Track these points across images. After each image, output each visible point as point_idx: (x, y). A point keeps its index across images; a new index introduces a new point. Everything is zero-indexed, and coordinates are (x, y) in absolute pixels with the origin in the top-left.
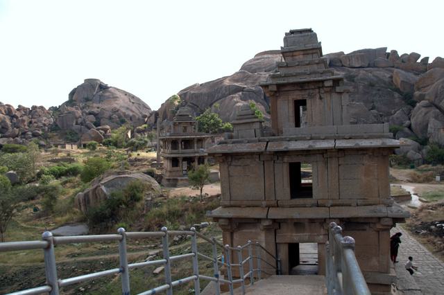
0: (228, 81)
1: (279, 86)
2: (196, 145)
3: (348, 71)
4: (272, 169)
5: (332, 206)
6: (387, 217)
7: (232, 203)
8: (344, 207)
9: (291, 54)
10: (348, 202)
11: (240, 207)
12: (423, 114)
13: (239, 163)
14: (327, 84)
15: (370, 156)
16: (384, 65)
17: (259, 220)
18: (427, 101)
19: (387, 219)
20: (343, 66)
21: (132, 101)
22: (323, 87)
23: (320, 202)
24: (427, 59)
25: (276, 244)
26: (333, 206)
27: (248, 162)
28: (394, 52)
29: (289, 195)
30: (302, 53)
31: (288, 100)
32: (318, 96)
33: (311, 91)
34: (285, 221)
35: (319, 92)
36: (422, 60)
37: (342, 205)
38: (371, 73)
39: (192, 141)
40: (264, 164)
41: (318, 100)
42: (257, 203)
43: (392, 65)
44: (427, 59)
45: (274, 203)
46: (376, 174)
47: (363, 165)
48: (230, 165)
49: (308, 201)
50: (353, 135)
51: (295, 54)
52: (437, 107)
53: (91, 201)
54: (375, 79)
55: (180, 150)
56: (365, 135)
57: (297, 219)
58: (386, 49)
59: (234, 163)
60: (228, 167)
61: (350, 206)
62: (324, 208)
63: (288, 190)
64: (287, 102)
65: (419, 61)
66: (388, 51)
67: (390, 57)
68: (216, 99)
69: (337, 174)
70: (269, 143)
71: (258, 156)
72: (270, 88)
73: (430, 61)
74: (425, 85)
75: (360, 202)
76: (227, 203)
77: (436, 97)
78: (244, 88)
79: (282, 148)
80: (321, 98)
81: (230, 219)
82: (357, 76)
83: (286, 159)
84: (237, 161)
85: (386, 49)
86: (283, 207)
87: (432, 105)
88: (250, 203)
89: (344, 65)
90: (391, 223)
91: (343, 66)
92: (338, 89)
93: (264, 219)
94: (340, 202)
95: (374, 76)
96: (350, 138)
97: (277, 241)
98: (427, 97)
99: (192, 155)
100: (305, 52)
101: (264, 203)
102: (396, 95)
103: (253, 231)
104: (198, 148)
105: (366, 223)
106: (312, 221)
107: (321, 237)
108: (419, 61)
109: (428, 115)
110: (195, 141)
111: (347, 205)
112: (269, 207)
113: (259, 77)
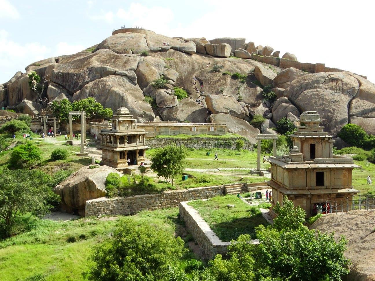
7: (294, 188)
12: (282, 109)
13: (297, 172)
14: (327, 139)
16: (241, 55)
18: (286, 98)
24: (278, 53)
25: (311, 204)
26: (333, 189)
28: (252, 44)
33: (318, 141)
35: (321, 141)
36: (274, 54)
37: (335, 188)
38: (235, 64)
42: (304, 188)
43: (251, 57)
44: (278, 53)
49: (323, 187)
51: (310, 123)
53: (80, 192)
54: (239, 71)
58: (244, 40)
59: (294, 172)
65: (272, 54)
66: (247, 42)
67: (248, 48)
73: (281, 56)
76: (292, 188)
77: (292, 94)
80: (321, 144)
85: (244, 40)
86: (314, 189)
87: (291, 101)
88: (301, 188)
98: (285, 94)
99: (135, 148)
101: (307, 188)
103: (301, 199)
105: (343, 195)
106: (325, 194)
107: (328, 201)
108: (272, 54)
109: (287, 109)
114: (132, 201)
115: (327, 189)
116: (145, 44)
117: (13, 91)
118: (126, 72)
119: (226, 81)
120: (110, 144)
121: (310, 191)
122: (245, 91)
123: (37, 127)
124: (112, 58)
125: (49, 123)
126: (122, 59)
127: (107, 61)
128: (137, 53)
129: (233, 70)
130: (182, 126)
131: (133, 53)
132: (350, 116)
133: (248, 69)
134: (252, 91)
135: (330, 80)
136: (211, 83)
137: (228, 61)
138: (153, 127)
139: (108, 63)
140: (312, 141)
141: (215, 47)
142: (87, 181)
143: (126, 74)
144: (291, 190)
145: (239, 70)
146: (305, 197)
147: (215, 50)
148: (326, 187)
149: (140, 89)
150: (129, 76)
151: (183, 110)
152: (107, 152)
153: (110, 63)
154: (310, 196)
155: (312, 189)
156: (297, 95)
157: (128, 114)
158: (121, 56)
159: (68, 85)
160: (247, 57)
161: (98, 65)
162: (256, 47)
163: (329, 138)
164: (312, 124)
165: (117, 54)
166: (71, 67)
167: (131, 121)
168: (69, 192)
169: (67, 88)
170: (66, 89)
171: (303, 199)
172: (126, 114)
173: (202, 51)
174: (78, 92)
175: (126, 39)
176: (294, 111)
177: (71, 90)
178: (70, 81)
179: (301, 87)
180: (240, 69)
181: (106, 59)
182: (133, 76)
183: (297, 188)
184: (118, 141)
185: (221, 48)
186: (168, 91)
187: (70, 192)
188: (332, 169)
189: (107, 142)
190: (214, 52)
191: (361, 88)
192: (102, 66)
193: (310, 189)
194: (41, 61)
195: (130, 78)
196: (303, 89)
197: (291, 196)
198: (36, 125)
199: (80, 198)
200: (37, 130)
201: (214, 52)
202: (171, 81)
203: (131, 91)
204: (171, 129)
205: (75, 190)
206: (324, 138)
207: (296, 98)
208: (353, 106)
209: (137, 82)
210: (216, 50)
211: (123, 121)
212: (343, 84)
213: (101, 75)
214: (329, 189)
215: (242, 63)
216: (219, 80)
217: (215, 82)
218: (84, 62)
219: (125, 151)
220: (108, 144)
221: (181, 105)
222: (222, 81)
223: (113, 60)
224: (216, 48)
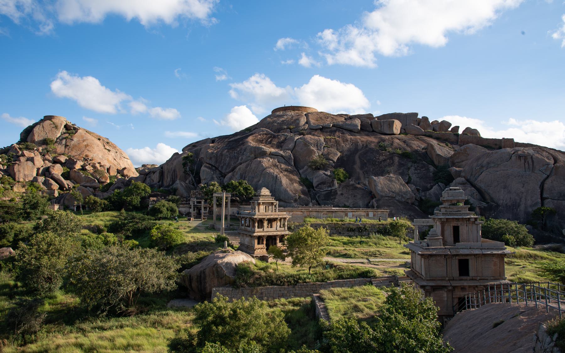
3: (381, 138)
7: (431, 278)
11: (435, 280)
15: (496, 257)
20: (373, 131)
21: (108, 147)
24: (457, 128)
26: (480, 280)
27: (439, 258)
28: (425, 119)
31: (450, 226)
32: (465, 224)
35: (466, 223)
36: (452, 129)
37: (484, 279)
40: (446, 260)
41: (465, 227)
43: (424, 134)
44: (457, 128)
45: (452, 278)
49: (468, 278)
50: (489, 247)
52: (473, 185)
53: (207, 278)
56: (495, 248)
58: (416, 114)
62: (475, 281)
63: (458, 272)
65: (450, 129)
66: (420, 116)
67: (421, 124)
68: (239, 161)
72: (442, 220)
73: (460, 132)
74: (460, 160)
76: (429, 279)
77: (472, 175)
80: (467, 226)
81: (432, 286)
83: (457, 258)
85: (416, 114)
86: (456, 280)
88: (440, 278)
89: (375, 130)
91: (373, 131)
92: (476, 222)
94: (483, 278)
96: (488, 249)
97: (453, 297)
98: (463, 174)
99: (275, 233)
101: (447, 278)
102: (432, 168)
103: (441, 292)
106: (470, 287)
108: (450, 129)
111: (485, 280)
114: (263, 291)
115: (472, 280)
119: (393, 161)
120: (248, 228)
121: (451, 282)
122: (416, 172)
123: (186, 210)
125: (197, 205)
130: (335, 211)
132: (543, 199)
134: (424, 172)
135: (518, 158)
138: (302, 211)
139: (263, 143)
140: (455, 222)
141: (382, 124)
142: (216, 266)
143: (281, 154)
144: (427, 280)
146: (446, 290)
147: (383, 127)
148: (471, 278)
150: (285, 157)
151: (342, 194)
152: (245, 237)
154: (450, 288)
155: (453, 280)
156: (477, 175)
157: (268, 196)
159: (221, 166)
160: (420, 134)
162: (430, 122)
163: (476, 219)
167: (272, 203)
168: (196, 277)
169: (220, 169)
170: (219, 171)
172: (266, 196)
173: (368, 129)
174: (230, 174)
176: (473, 193)
177: (223, 171)
178: (223, 162)
179: (482, 166)
184: (256, 225)
185: (389, 124)
186: (326, 173)
187: (197, 276)
189: (245, 226)
191: (558, 164)
193: (451, 280)
195: (285, 159)
196: (484, 169)
197: (427, 288)
198: (185, 207)
199: (208, 284)
200: (186, 213)
203: (286, 173)
204: (323, 214)
205: (202, 275)
206: (469, 219)
207: (476, 179)
208: (546, 186)
210: (384, 127)
211: (262, 203)
212: (533, 161)
213: (255, 156)
214: (476, 280)
216: (385, 160)
217: (381, 162)
219: (264, 236)
220: (246, 227)
221: (341, 189)
222: (388, 161)
224: (383, 125)
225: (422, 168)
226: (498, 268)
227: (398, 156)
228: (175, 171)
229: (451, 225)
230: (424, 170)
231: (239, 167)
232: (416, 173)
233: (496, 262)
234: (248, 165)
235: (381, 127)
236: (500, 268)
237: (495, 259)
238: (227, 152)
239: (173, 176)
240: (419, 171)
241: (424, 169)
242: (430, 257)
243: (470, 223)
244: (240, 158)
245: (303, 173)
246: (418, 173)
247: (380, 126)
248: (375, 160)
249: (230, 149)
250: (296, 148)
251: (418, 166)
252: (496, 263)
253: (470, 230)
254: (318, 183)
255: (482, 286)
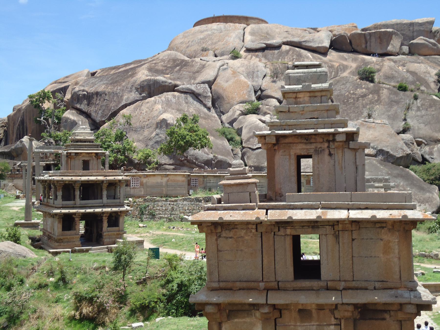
0: (146, 72)
1: (278, 137)
2: (105, 193)
3: (363, 60)
4: (271, 242)
5: (344, 289)
6: (410, 304)
7: (222, 285)
8: (359, 291)
9: (294, 95)
10: (364, 284)
11: (230, 289)
15: (389, 230)
17: (255, 306)
19: (410, 306)
22: (334, 140)
23: (330, 284)
27: (242, 233)
29: (293, 274)
30: (308, 94)
31: (290, 155)
32: (327, 152)
33: (319, 146)
34: (287, 307)
35: (328, 147)
38: (404, 65)
39: (99, 184)
40: (262, 237)
41: (326, 157)
42: (252, 285)
45: (274, 285)
46: (397, 251)
47: (381, 240)
48: (220, 236)
51: (300, 95)
55: (78, 201)
57: (302, 305)
59: (224, 234)
60: (217, 240)
61: (366, 289)
64: (288, 157)
68: (123, 103)
69: (350, 250)
70: (269, 211)
71: (254, 227)
75: (378, 285)
76: (215, 285)
78: (176, 86)
79: (285, 218)
80: (330, 154)
82: (379, 70)
83: (289, 231)
84: (227, 231)
86: (285, 290)
88: (244, 285)
90: (414, 311)
93: (263, 305)
94: (354, 284)
95: (408, 71)
100: (312, 94)
101: (262, 285)
103: (248, 320)
104: (108, 197)
105: (385, 311)
106: (320, 308)
110: (105, 186)
111: (361, 289)
112: (267, 290)
113: (203, 66)
115: (328, 289)
116: (240, 39)
117: (14, 124)
118: (193, 88)
119: (379, 96)
122: (419, 113)
124: (177, 65)
126: (193, 66)
127: (166, 70)
128: (222, 54)
129: (396, 75)
131: (216, 56)
133: (429, 73)
134: (433, 113)
136: (348, 101)
137: (392, 60)
139: (168, 74)
141: (368, 37)
143: (192, 90)
145: (409, 74)
147: (368, 43)
148: (321, 284)
149: (216, 116)
153: (171, 74)
155: (279, 289)
158: (193, 61)
161: (147, 76)
164: (307, 99)
165: (187, 59)
166: (105, 82)
171: (253, 319)
172: (85, 141)
173: (344, 47)
175: (209, 32)
180: (413, 73)
181: (165, 66)
182: (205, 94)
183: (229, 285)
184: (60, 194)
185: (380, 37)
186: (263, 118)
188: (340, 226)
190: (366, 47)
192: (152, 78)
193: (273, 289)
194: (67, 77)
201: (366, 47)
202: (274, 100)
209: (210, 104)
210: (370, 42)
214: (336, 290)
215: (419, 63)
216: (364, 96)
217: (358, 98)
218: (129, 72)
222: (370, 96)
223: (178, 68)
224: (370, 38)
225: (431, 106)
226: (396, 260)
227: (388, 89)
228: (22, 122)
229: (293, 152)
230: (433, 111)
231: (121, 112)
232: (418, 116)
233: (389, 242)
234: (136, 109)
235: (366, 43)
236: (399, 259)
237: (386, 236)
238: (105, 87)
239: (20, 132)
240: (423, 112)
241: (433, 109)
242: (219, 230)
243: (337, 148)
244: (125, 97)
245: (227, 119)
246: (422, 116)
247: (363, 41)
248: (348, 95)
249: (111, 84)
250: (218, 80)
251: (422, 105)
252: (391, 244)
253: (337, 163)
254: (248, 136)
255: (347, 307)
